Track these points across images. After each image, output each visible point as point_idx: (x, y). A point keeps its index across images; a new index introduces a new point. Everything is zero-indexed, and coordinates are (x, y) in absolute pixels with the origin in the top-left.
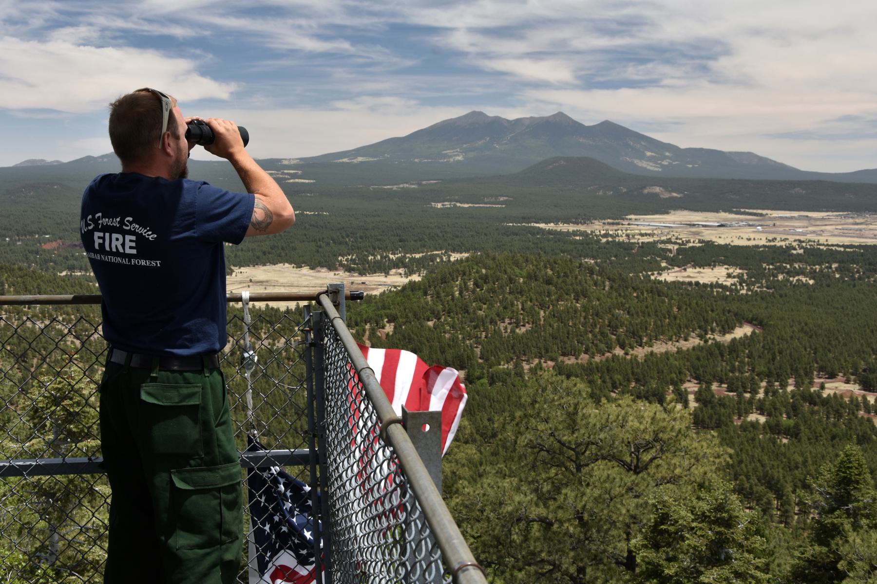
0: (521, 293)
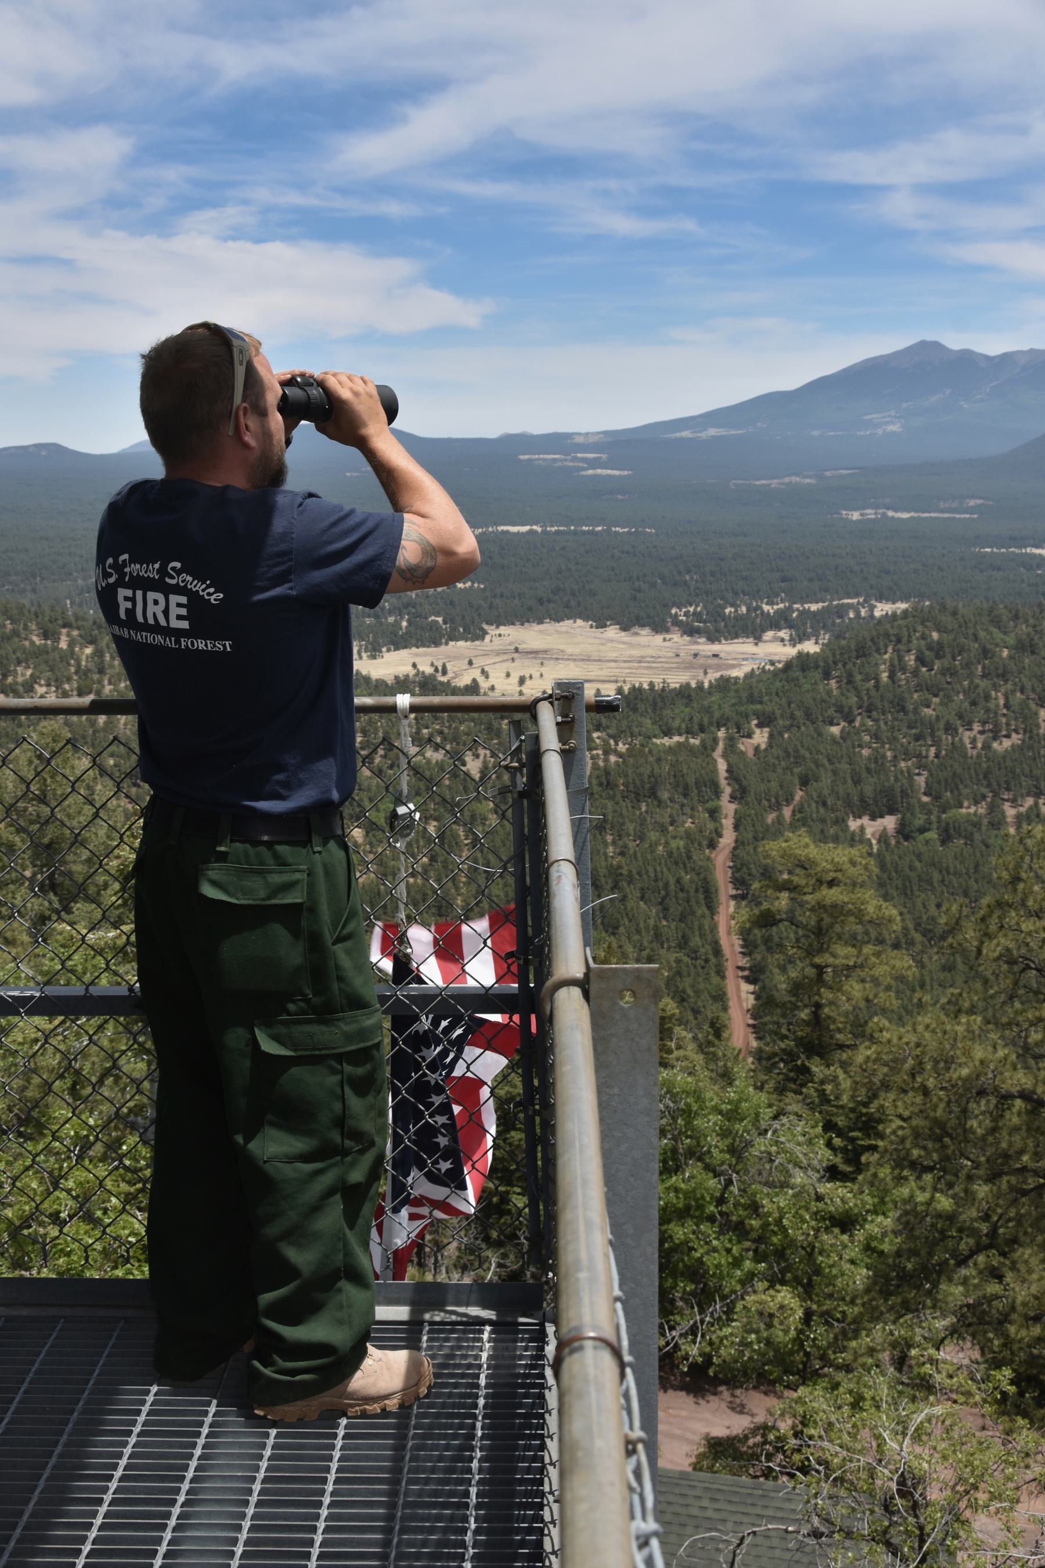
0: (1004, 676)
